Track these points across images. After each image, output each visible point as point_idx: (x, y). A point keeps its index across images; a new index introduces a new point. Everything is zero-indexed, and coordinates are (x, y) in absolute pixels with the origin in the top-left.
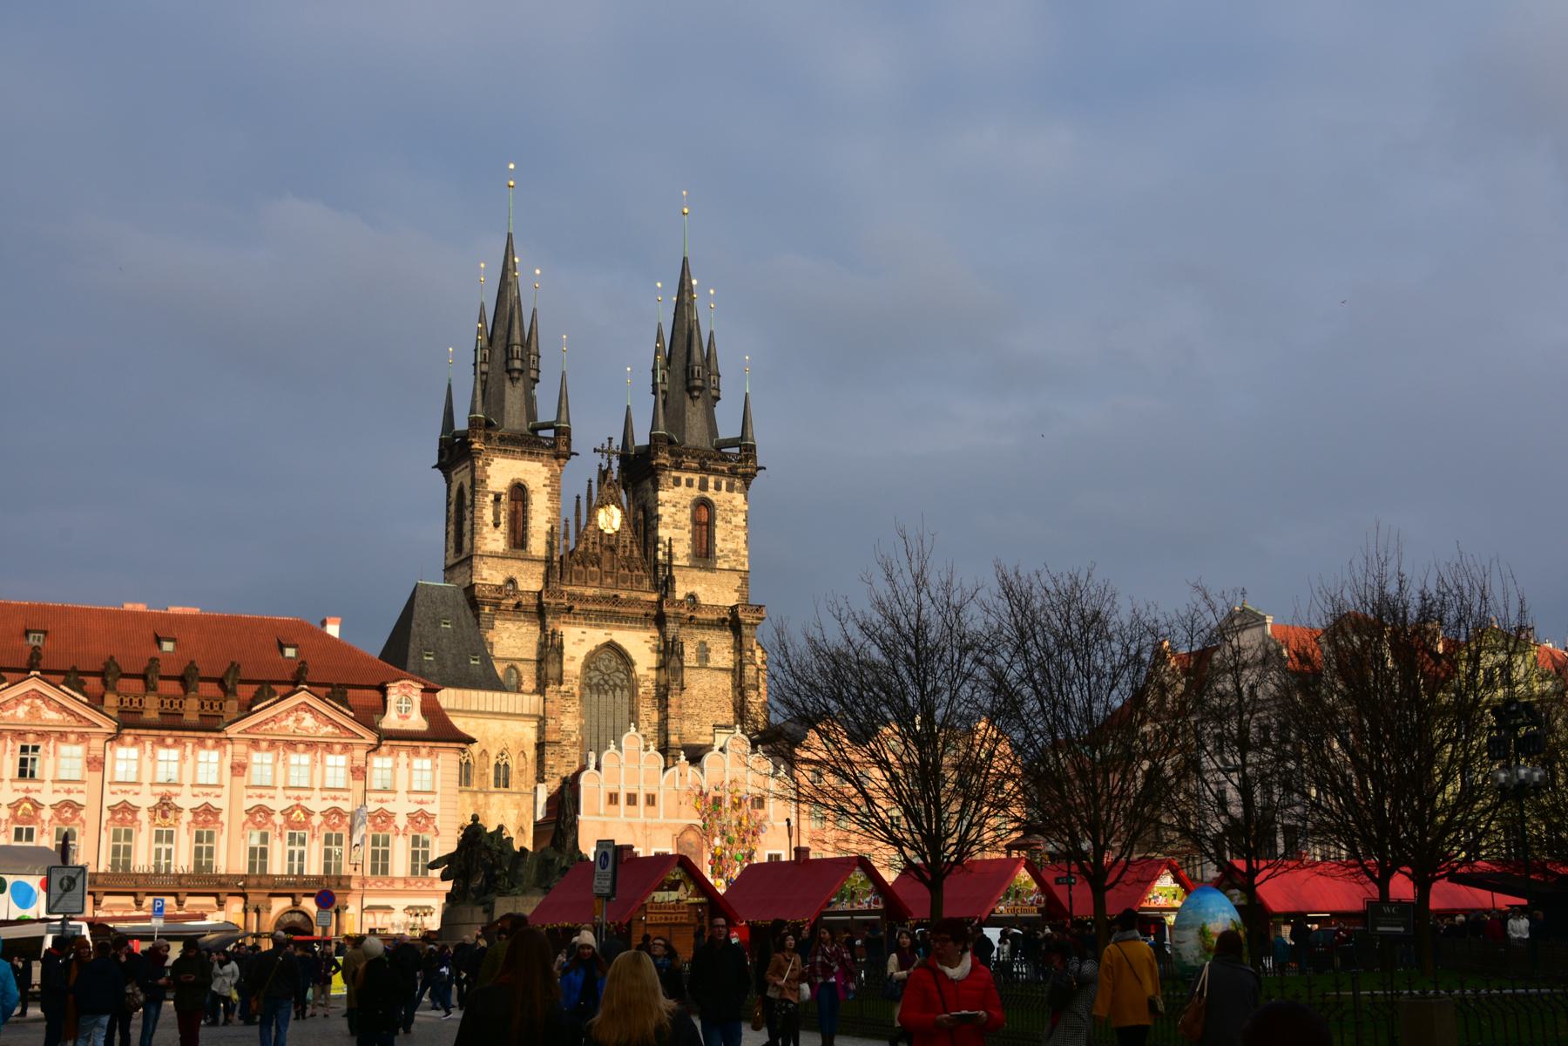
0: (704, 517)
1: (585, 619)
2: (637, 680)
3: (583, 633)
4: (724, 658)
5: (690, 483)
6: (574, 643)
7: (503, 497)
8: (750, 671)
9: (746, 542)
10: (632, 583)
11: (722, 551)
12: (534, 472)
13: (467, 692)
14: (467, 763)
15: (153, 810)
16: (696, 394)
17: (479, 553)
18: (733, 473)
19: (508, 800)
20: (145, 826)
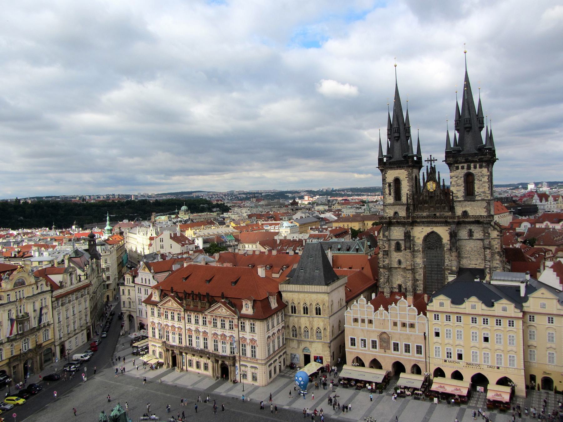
0: (469, 180)
1: (423, 224)
2: (444, 245)
3: (423, 229)
4: (480, 235)
5: (463, 168)
6: (419, 233)
7: (392, 184)
9: (489, 188)
10: (441, 209)
11: (478, 193)
12: (402, 174)
13: (303, 286)
14: (307, 307)
15: (195, 331)
17: (385, 204)
18: (481, 161)
19: (320, 319)
20: (194, 335)
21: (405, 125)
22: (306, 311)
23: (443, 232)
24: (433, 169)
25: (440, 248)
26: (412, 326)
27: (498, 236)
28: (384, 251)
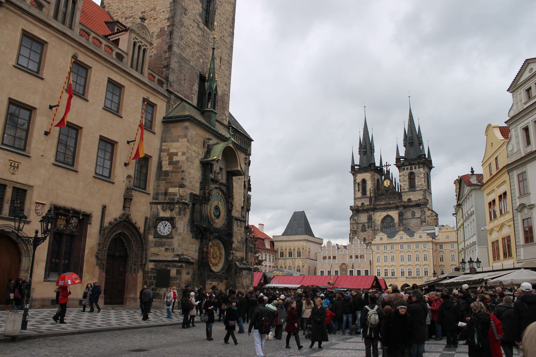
0: (412, 177)
5: (407, 169)
8: (423, 218)
9: (424, 181)
12: (367, 176)
13: (289, 236)
14: (291, 252)
16: (411, 144)
18: (419, 163)
19: (300, 260)
21: (370, 144)
22: (290, 254)
23: (394, 214)
24: (388, 172)
25: (393, 227)
26: (362, 257)
27: (432, 214)
28: (353, 230)
